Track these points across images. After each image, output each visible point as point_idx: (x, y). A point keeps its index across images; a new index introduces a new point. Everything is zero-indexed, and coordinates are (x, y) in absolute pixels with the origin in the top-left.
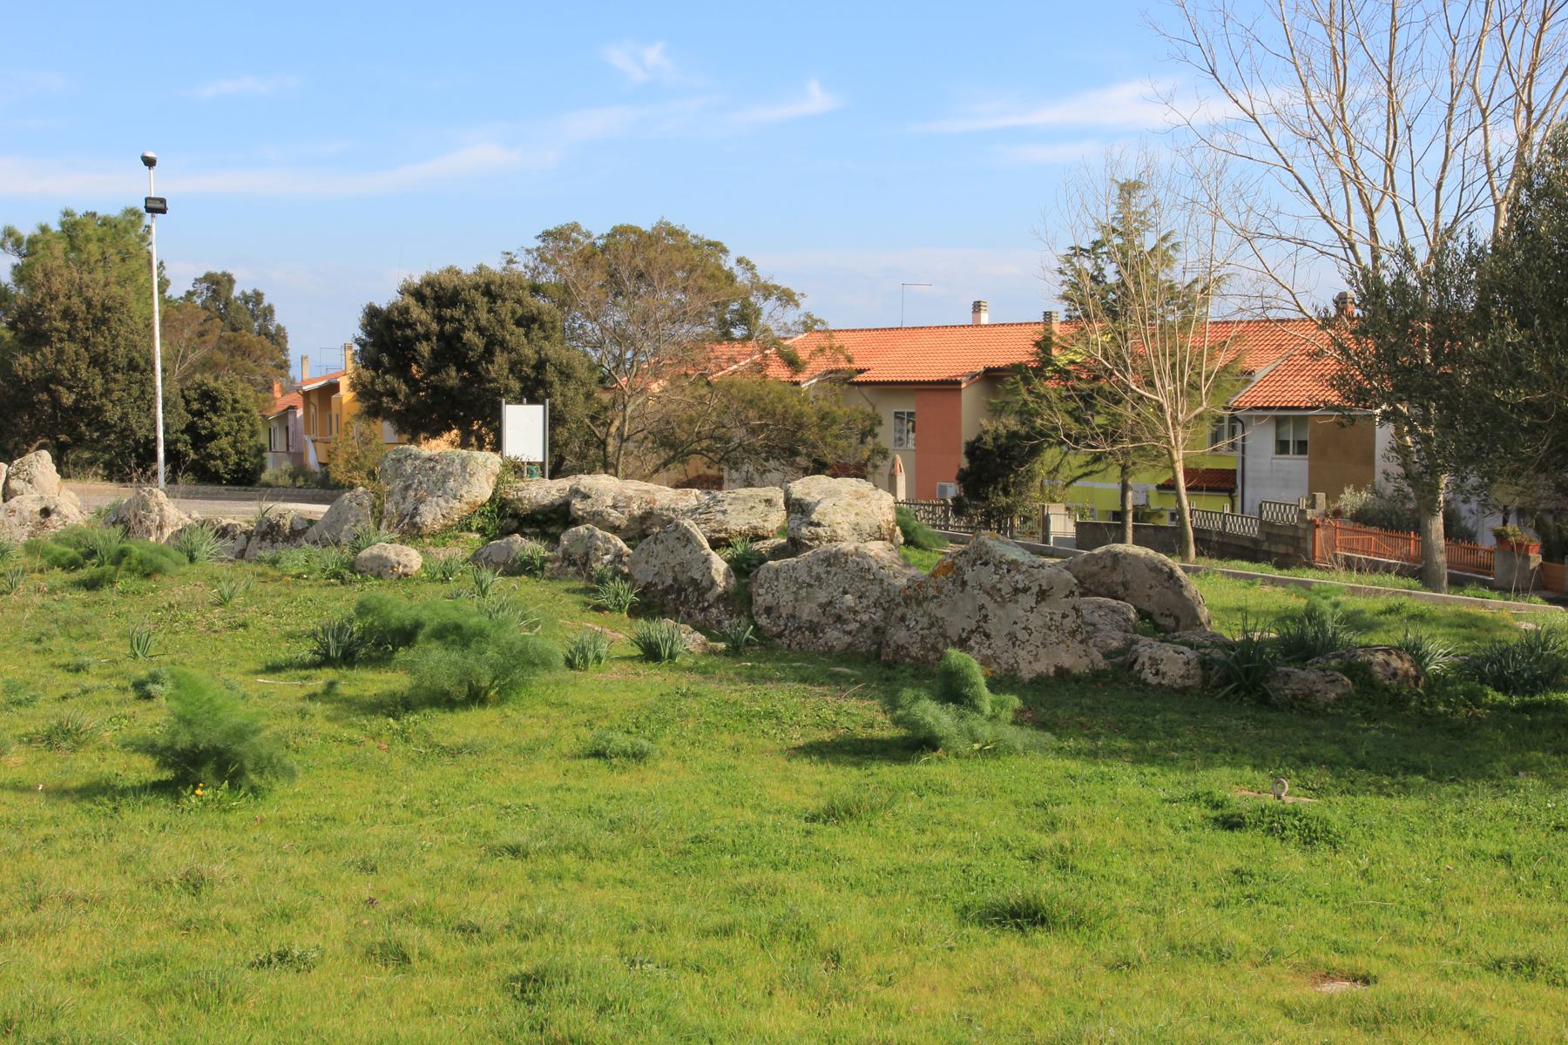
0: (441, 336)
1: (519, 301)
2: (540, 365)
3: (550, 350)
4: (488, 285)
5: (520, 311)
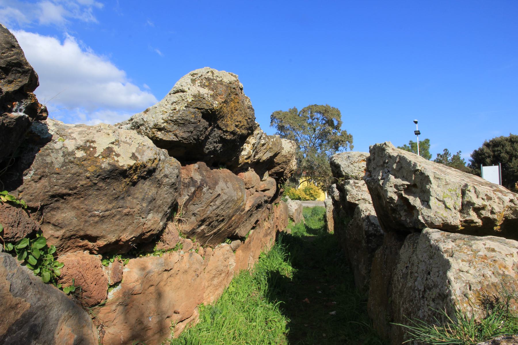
0: (494, 156)
4: (511, 139)
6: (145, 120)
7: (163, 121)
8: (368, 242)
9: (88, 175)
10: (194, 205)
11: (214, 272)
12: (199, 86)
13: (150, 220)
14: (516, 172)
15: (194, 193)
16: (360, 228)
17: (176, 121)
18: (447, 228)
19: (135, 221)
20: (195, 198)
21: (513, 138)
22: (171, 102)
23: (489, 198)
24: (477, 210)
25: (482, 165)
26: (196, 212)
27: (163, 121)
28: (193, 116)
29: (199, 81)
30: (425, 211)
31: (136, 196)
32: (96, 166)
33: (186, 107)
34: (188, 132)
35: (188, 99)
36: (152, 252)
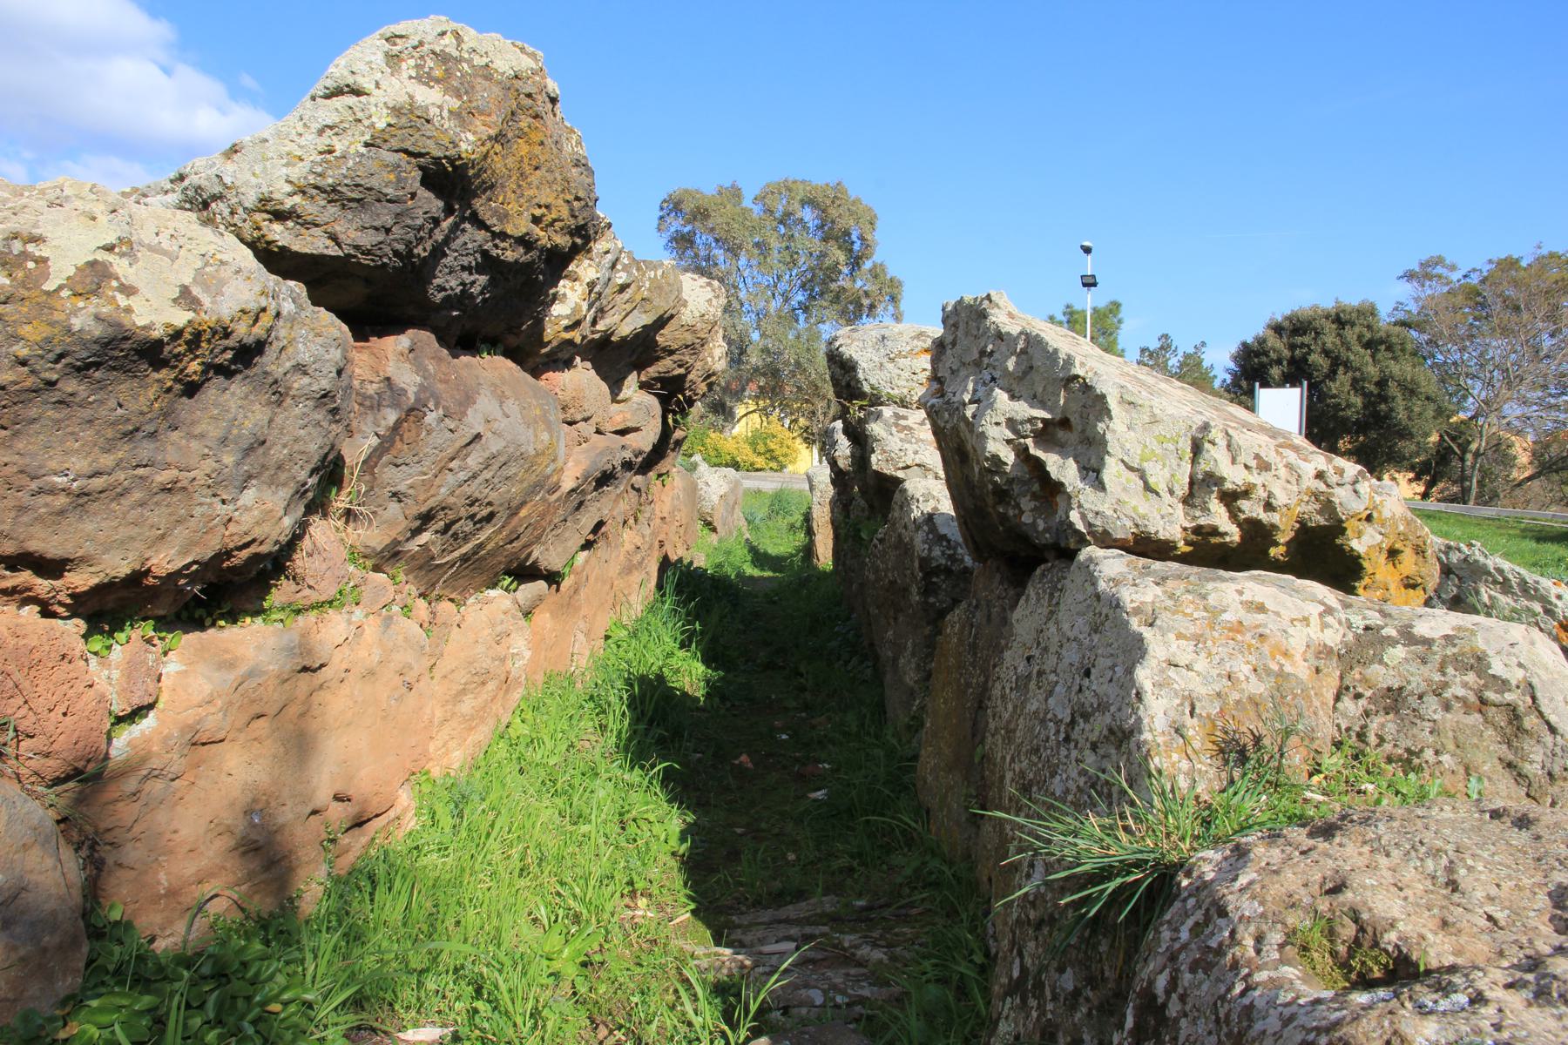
0: (1292, 361)
1: (1369, 327)
2: (1382, 383)
3: (1395, 368)
4: (1337, 315)
5: (1368, 336)
6: (228, 180)
7: (288, 188)
8: (928, 590)
9: (23, 352)
10: (397, 466)
11: (462, 677)
12: (411, 77)
13: (247, 509)
14: (1343, 410)
15: (396, 428)
16: (905, 548)
17: (334, 190)
18: (1146, 547)
19: (198, 511)
20: (398, 444)
21: (1344, 311)
22: (315, 126)
23: (1264, 467)
24: (1230, 499)
25: (1257, 384)
26: (402, 488)
27: (288, 188)
28: (392, 177)
29: (412, 62)
30: (1088, 498)
31: (197, 430)
32: (52, 324)
33: (367, 145)
34: (376, 229)
35: (374, 119)
36: (259, 612)
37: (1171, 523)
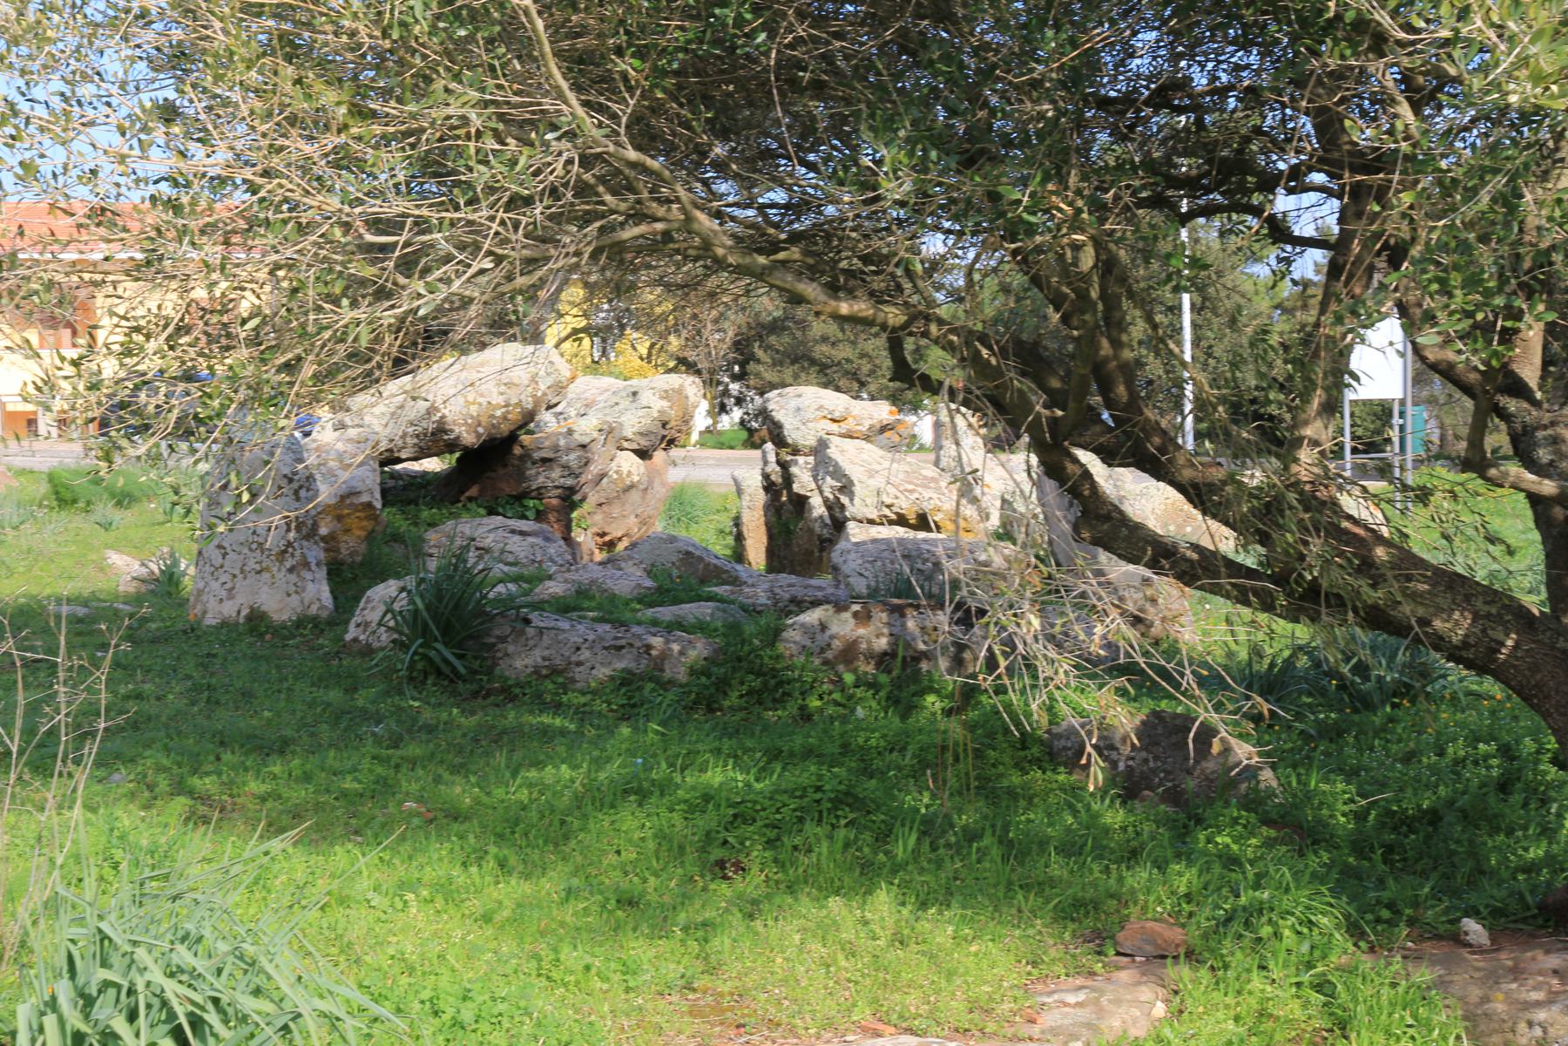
16: (811, 531)
24: (889, 506)
37: (874, 515)
